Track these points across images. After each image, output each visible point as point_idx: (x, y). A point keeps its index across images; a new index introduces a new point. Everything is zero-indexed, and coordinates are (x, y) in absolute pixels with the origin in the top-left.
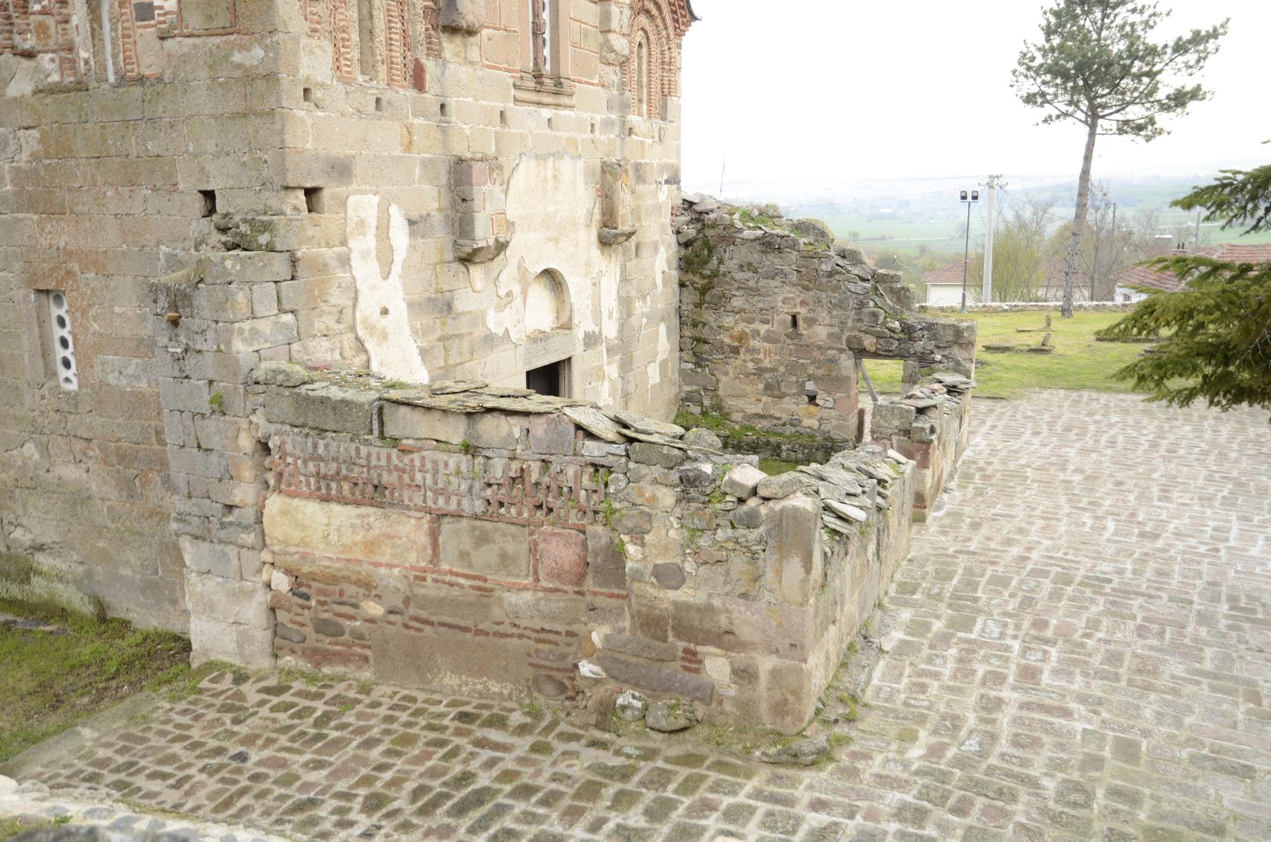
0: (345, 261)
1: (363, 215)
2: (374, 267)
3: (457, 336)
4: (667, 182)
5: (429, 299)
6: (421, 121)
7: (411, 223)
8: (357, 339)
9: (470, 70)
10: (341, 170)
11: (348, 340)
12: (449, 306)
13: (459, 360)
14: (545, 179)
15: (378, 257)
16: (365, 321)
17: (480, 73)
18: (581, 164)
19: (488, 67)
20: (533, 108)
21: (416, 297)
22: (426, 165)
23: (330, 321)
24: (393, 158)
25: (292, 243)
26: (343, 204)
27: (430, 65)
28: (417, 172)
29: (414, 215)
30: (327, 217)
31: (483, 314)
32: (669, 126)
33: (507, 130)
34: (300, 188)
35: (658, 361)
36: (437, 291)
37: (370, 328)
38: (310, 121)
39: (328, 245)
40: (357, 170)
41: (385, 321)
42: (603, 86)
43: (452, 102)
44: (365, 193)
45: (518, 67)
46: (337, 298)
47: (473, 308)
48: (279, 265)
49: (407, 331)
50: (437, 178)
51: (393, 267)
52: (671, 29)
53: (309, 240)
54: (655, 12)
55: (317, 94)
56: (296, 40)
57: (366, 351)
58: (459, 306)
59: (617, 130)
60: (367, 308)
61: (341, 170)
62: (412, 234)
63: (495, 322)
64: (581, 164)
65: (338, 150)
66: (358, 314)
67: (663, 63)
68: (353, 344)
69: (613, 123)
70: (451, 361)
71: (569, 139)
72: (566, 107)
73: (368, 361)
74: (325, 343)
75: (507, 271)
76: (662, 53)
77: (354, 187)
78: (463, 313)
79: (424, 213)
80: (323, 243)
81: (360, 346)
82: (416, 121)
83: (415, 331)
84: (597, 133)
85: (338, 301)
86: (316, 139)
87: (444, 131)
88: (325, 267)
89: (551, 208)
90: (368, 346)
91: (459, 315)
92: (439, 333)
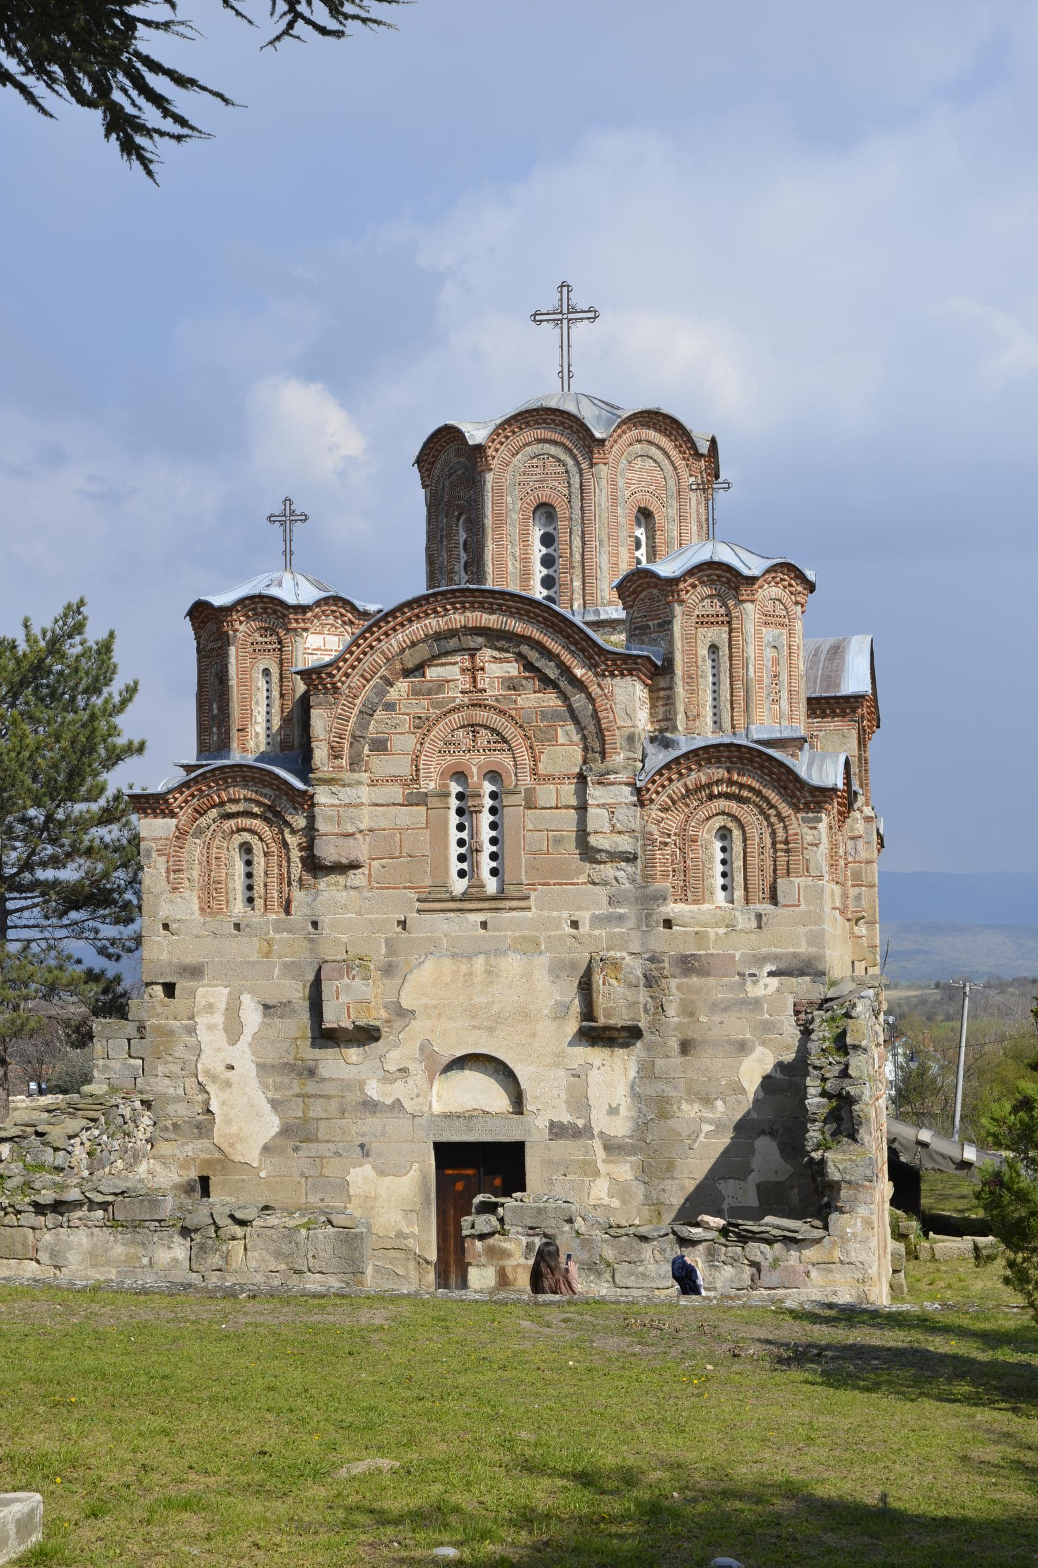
0: (192, 1030)
1: (211, 1000)
2: (221, 1037)
3: (322, 1096)
4: (771, 974)
5: (285, 1064)
6: (285, 935)
7: (266, 1007)
8: (199, 1084)
9: (353, 893)
10: (195, 972)
11: (190, 1083)
12: (312, 1072)
13: (322, 1115)
14: (470, 974)
15: (225, 1029)
16: (207, 1072)
17: (367, 894)
18: (543, 961)
19: (378, 888)
20: (452, 914)
21: (269, 1061)
22: (285, 965)
23: (176, 1069)
24: (248, 963)
25: (143, 1015)
26: (193, 993)
27: (298, 896)
28: (276, 970)
29: (270, 1002)
30: (178, 1003)
31: (362, 1084)
32: (779, 910)
33: (405, 935)
34: (156, 984)
35: (753, 1179)
36: (296, 1059)
37: (214, 1078)
38: (165, 943)
39: (175, 1018)
40: (208, 971)
41: (230, 1074)
42: (594, 884)
43: (325, 920)
44: (216, 986)
45: (429, 883)
46: (179, 1051)
47: (346, 1077)
48: (130, 1028)
49: (255, 1083)
50: (302, 975)
51: (242, 1037)
52: (786, 810)
53: (158, 1015)
54: (745, 793)
55: (173, 926)
56: (158, 896)
57: (208, 1093)
58: (324, 1071)
59: (631, 923)
60: (211, 1060)
61: (195, 972)
62: (265, 1015)
63: (374, 1090)
64: (543, 961)
65: (191, 959)
66: (199, 1066)
67: (774, 844)
68: (195, 1086)
69: (621, 918)
70: (311, 1114)
71: (524, 938)
72: (512, 909)
73: (209, 1099)
74: (167, 1081)
75: (398, 1051)
76: (773, 833)
77: (206, 982)
78: (331, 1079)
79: (284, 1001)
80: (170, 1017)
81: (202, 1088)
82: (277, 936)
83: (264, 1086)
84: (584, 929)
85: (182, 1056)
86: (169, 953)
87: (311, 940)
88: (171, 1033)
89: (480, 1000)
90: (208, 1089)
91: (324, 1080)
92: (297, 1091)
